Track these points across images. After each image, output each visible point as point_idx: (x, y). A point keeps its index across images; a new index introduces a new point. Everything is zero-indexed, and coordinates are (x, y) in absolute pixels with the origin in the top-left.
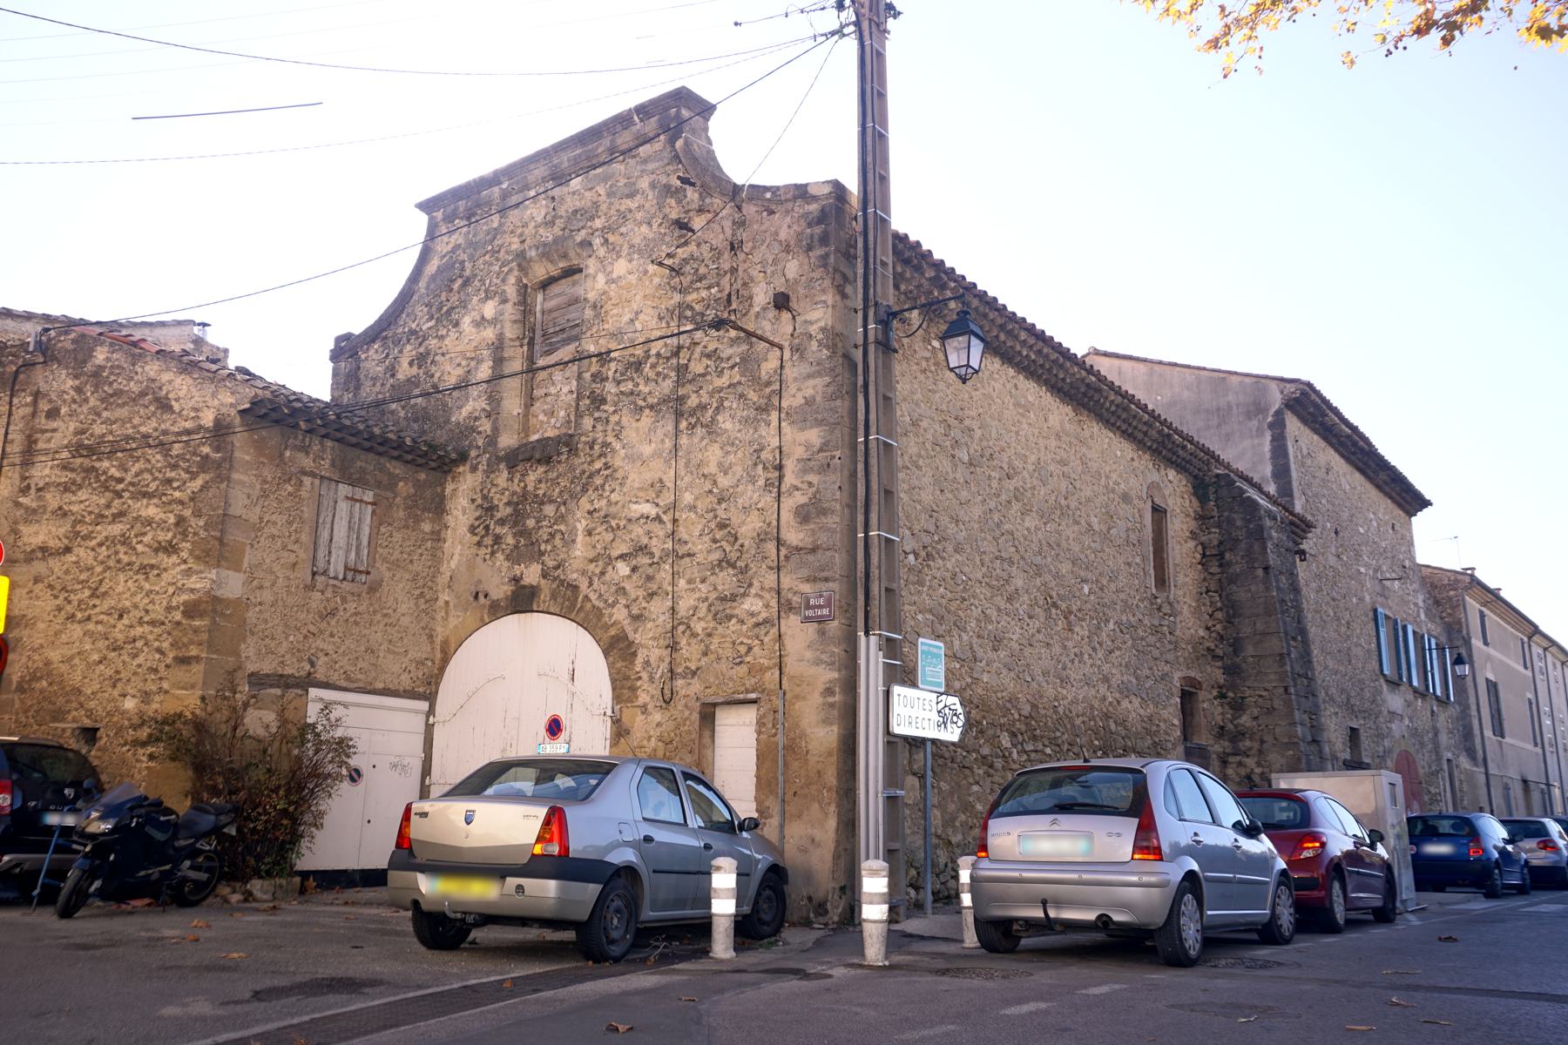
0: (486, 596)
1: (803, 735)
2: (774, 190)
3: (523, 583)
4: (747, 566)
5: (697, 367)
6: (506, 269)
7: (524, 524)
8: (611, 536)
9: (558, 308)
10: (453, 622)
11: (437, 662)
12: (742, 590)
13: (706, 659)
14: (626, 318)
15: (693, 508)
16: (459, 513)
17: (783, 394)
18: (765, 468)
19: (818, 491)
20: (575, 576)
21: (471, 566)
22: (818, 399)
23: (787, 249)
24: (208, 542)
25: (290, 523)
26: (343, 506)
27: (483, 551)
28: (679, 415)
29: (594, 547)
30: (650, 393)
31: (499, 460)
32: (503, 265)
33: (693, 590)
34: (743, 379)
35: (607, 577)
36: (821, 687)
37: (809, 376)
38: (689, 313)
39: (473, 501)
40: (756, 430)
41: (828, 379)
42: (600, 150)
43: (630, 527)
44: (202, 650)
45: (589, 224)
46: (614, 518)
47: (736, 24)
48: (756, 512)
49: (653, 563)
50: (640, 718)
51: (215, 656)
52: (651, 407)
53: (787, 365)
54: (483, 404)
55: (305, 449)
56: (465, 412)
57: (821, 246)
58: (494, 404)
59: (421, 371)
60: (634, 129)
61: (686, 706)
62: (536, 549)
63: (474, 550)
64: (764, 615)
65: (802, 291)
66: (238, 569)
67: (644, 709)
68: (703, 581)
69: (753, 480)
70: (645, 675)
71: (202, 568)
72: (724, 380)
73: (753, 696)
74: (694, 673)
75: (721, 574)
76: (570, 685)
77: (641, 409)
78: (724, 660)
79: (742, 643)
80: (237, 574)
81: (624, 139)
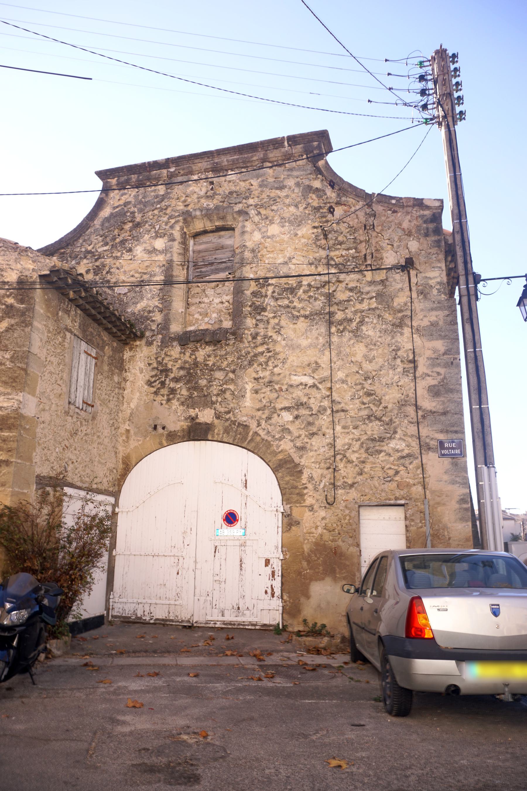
0: (164, 428)
1: (445, 527)
2: (399, 199)
3: (197, 421)
4: (391, 420)
5: (341, 296)
6: (173, 221)
7: (196, 383)
8: (275, 395)
9: (206, 251)
10: (133, 444)
11: (119, 470)
12: (389, 435)
13: (361, 477)
14: (280, 260)
15: (343, 382)
16: (138, 372)
17: (413, 318)
18: (402, 361)
19: (445, 378)
20: (245, 419)
21: (148, 407)
22: (441, 323)
23: (409, 234)
24: (15, 372)
25: (59, 364)
26: (83, 356)
27: (159, 398)
28: (330, 323)
29: (261, 401)
30: (303, 308)
31: (173, 339)
32: (171, 217)
33: (348, 433)
34: (380, 306)
35: (273, 421)
36: (457, 498)
37: (432, 309)
38: (333, 263)
39: (150, 364)
40: (393, 337)
41: (447, 312)
42: (255, 158)
43: (291, 390)
44: (11, 456)
45: (244, 201)
46: (277, 383)
47: (369, 101)
48: (396, 388)
49: (312, 414)
50: (308, 514)
51: (19, 461)
52: (306, 317)
53: (416, 301)
54: (156, 302)
55: (67, 312)
56: (140, 306)
57: (435, 235)
58: (165, 304)
59: (97, 278)
60: (283, 150)
61: (346, 507)
62: (209, 399)
63: (152, 396)
64: (406, 452)
65: (422, 259)
66: (34, 395)
67: (311, 508)
68: (356, 428)
69: (394, 368)
70: (310, 486)
71: (9, 390)
72: (364, 305)
73: (402, 502)
74: (352, 486)
75: (371, 424)
76: (244, 490)
77: (298, 317)
78: (376, 479)
79: (390, 468)
80: (33, 398)
81: (274, 154)
